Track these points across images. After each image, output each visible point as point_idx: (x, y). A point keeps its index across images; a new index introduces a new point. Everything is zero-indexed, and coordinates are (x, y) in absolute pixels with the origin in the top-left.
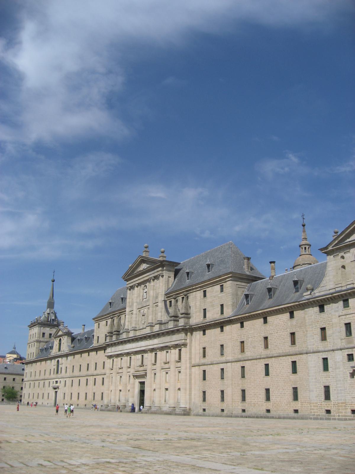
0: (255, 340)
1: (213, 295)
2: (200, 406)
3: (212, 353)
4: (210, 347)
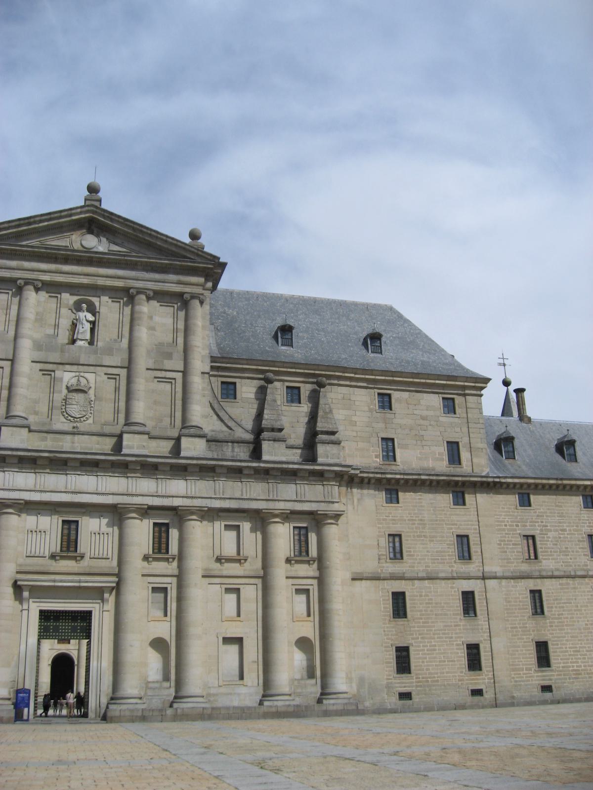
0: (564, 538)
1: (415, 412)
2: (388, 687)
3: (428, 552)
4: (418, 536)
